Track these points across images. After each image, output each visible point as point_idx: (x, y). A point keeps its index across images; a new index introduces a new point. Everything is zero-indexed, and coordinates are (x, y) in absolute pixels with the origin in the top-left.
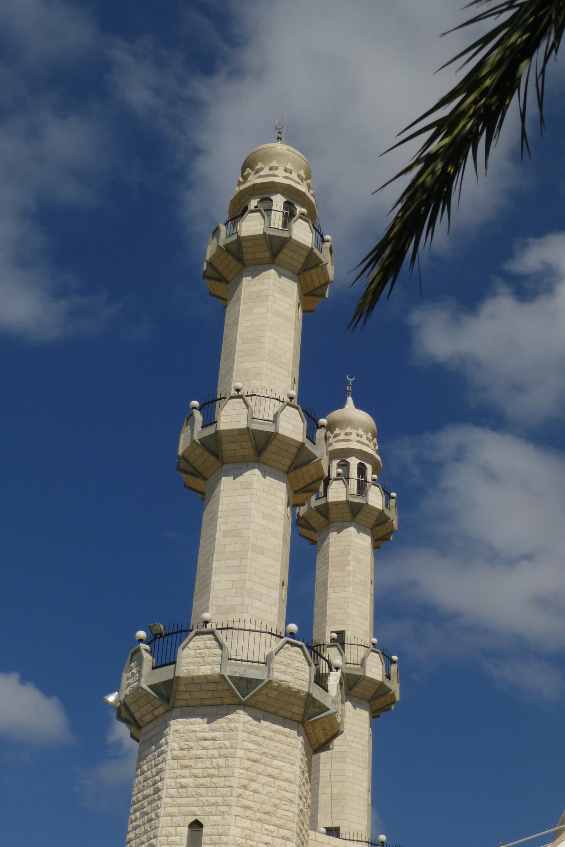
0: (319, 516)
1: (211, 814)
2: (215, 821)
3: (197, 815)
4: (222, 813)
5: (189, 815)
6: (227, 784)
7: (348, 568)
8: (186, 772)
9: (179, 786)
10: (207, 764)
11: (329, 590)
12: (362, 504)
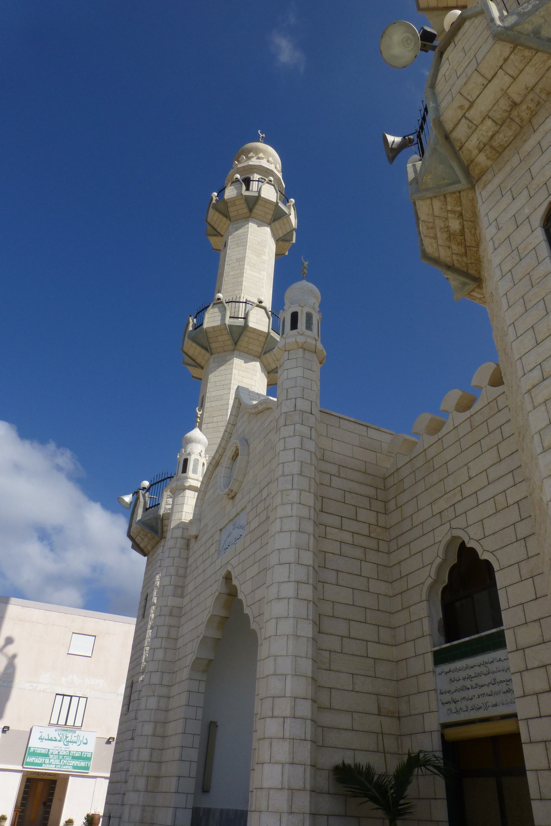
0: (244, 206)
7: (263, 257)
11: (246, 266)
12: (286, 214)
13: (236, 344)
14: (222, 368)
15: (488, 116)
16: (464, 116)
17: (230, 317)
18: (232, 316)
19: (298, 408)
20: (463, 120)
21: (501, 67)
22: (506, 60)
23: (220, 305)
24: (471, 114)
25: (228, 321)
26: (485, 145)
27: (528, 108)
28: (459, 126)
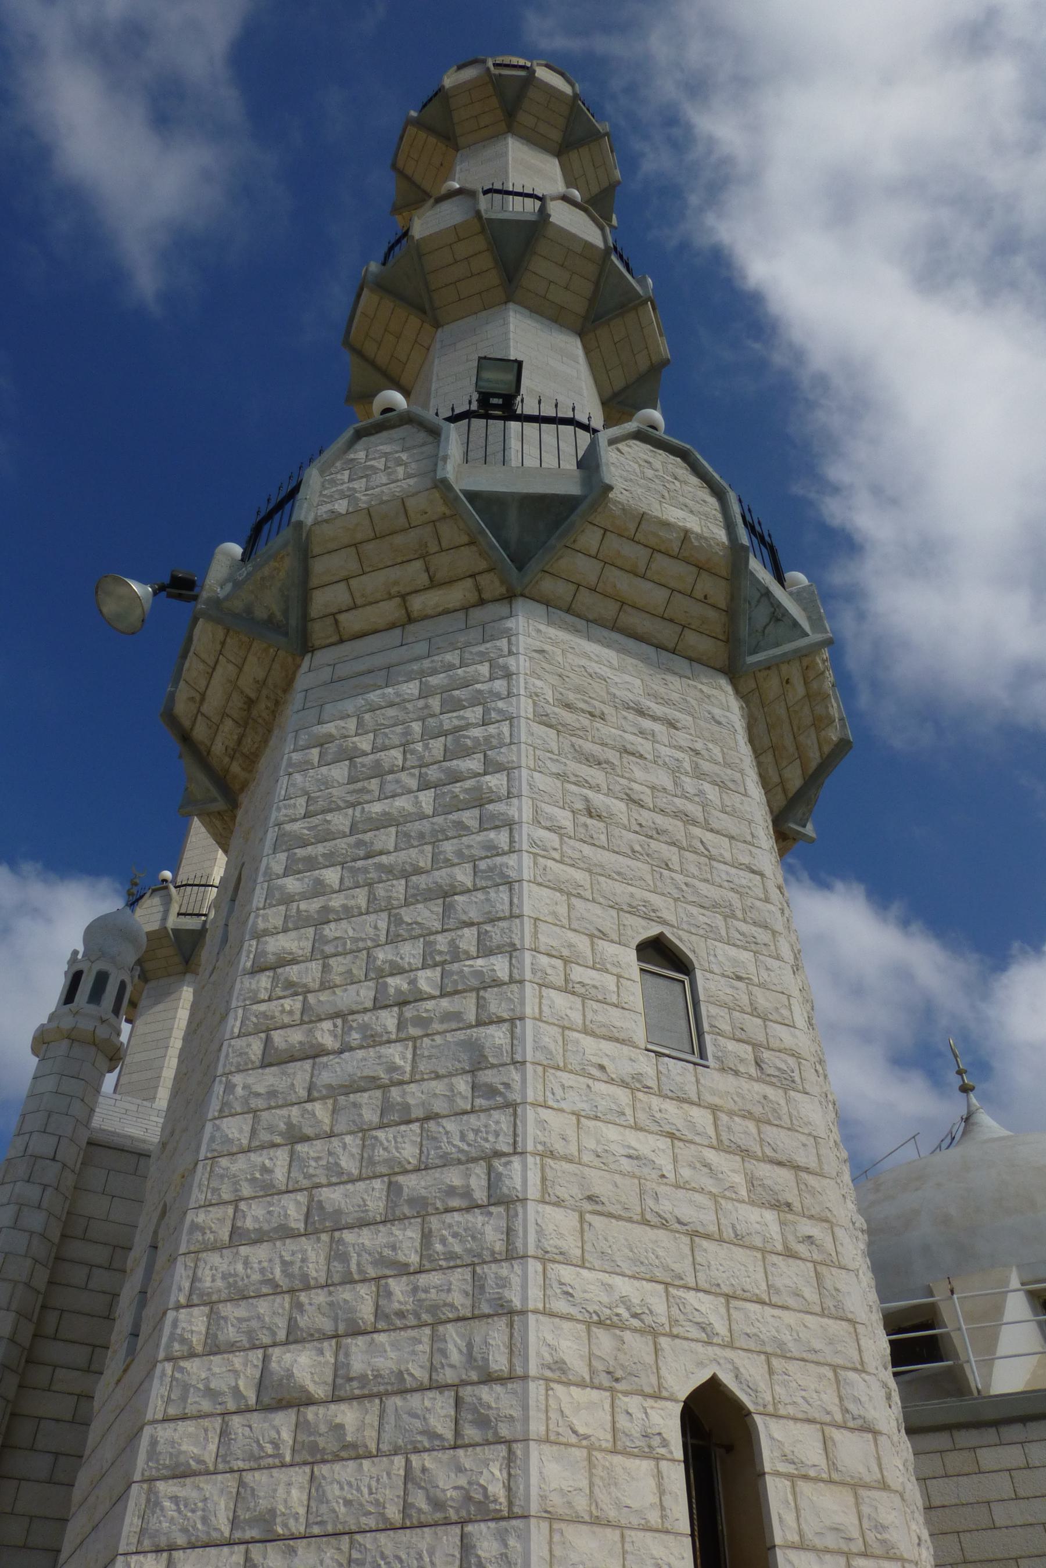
1: (710, 933)
2: (735, 962)
3: (665, 922)
4: (750, 944)
5: (633, 910)
6: (746, 860)
8: (596, 775)
9: (579, 805)
10: (664, 779)
13: (187, 962)
14: (160, 1007)
15: (224, 715)
16: (199, 711)
17: (179, 914)
18: (183, 911)
19: (29, 1151)
20: (199, 717)
21: (221, 653)
22: (223, 643)
23: (163, 892)
24: (205, 709)
25: (172, 922)
26: (235, 751)
27: (267, 708)
28: (197, 726)
